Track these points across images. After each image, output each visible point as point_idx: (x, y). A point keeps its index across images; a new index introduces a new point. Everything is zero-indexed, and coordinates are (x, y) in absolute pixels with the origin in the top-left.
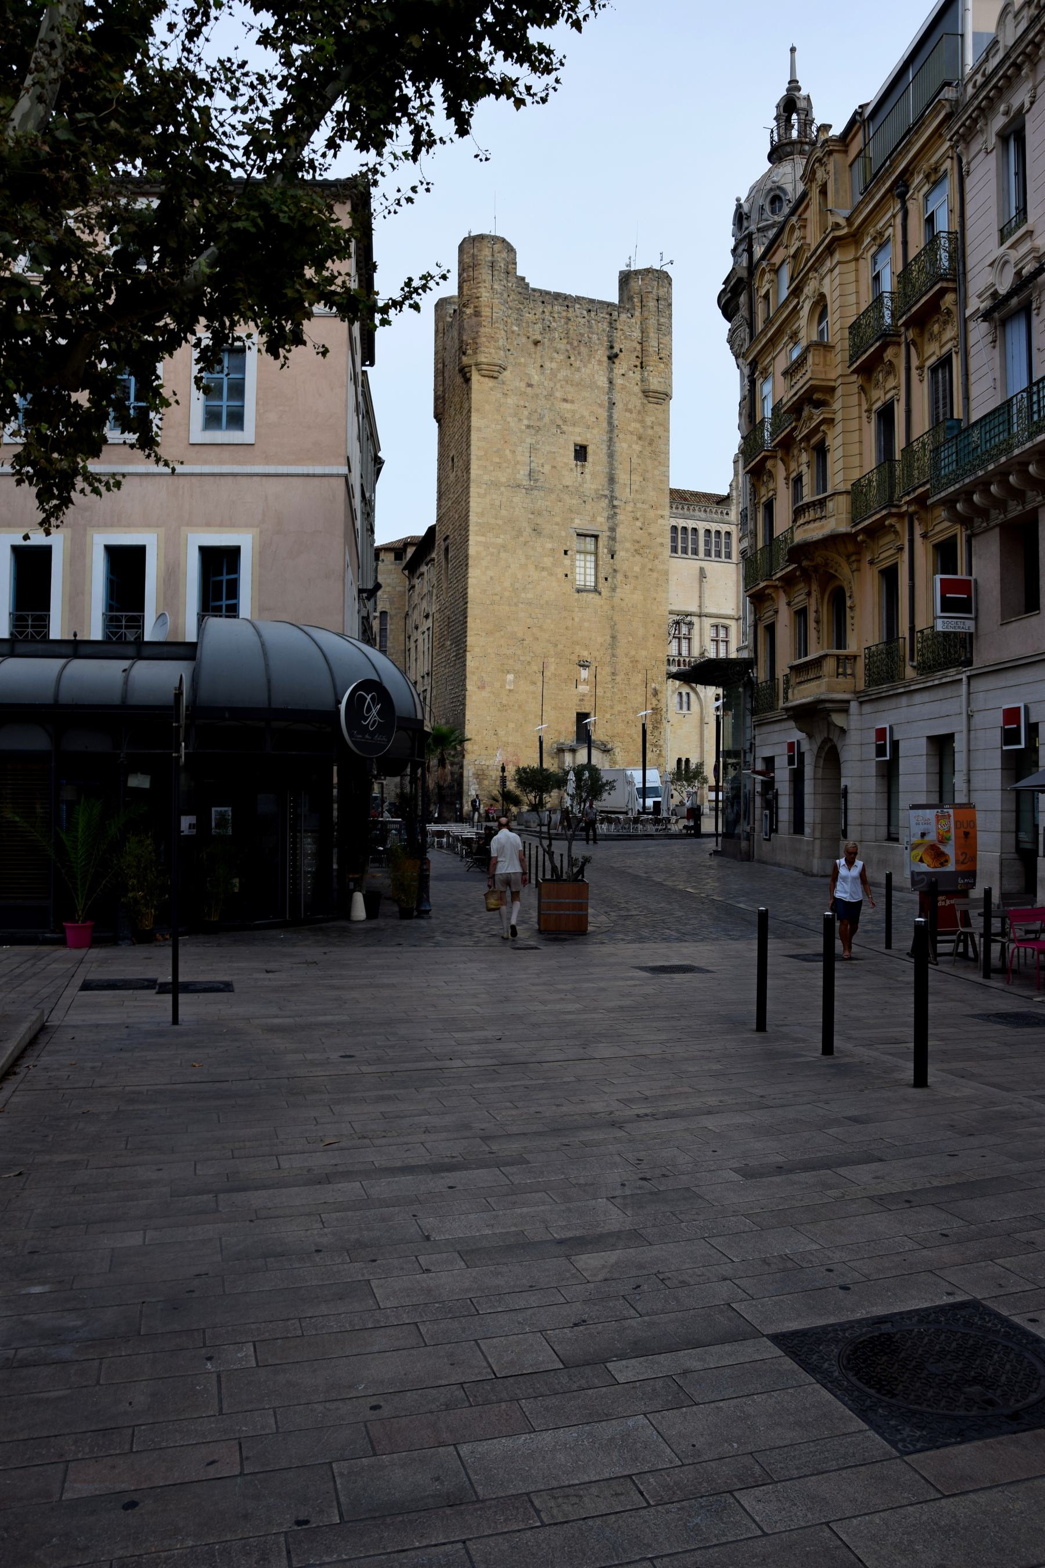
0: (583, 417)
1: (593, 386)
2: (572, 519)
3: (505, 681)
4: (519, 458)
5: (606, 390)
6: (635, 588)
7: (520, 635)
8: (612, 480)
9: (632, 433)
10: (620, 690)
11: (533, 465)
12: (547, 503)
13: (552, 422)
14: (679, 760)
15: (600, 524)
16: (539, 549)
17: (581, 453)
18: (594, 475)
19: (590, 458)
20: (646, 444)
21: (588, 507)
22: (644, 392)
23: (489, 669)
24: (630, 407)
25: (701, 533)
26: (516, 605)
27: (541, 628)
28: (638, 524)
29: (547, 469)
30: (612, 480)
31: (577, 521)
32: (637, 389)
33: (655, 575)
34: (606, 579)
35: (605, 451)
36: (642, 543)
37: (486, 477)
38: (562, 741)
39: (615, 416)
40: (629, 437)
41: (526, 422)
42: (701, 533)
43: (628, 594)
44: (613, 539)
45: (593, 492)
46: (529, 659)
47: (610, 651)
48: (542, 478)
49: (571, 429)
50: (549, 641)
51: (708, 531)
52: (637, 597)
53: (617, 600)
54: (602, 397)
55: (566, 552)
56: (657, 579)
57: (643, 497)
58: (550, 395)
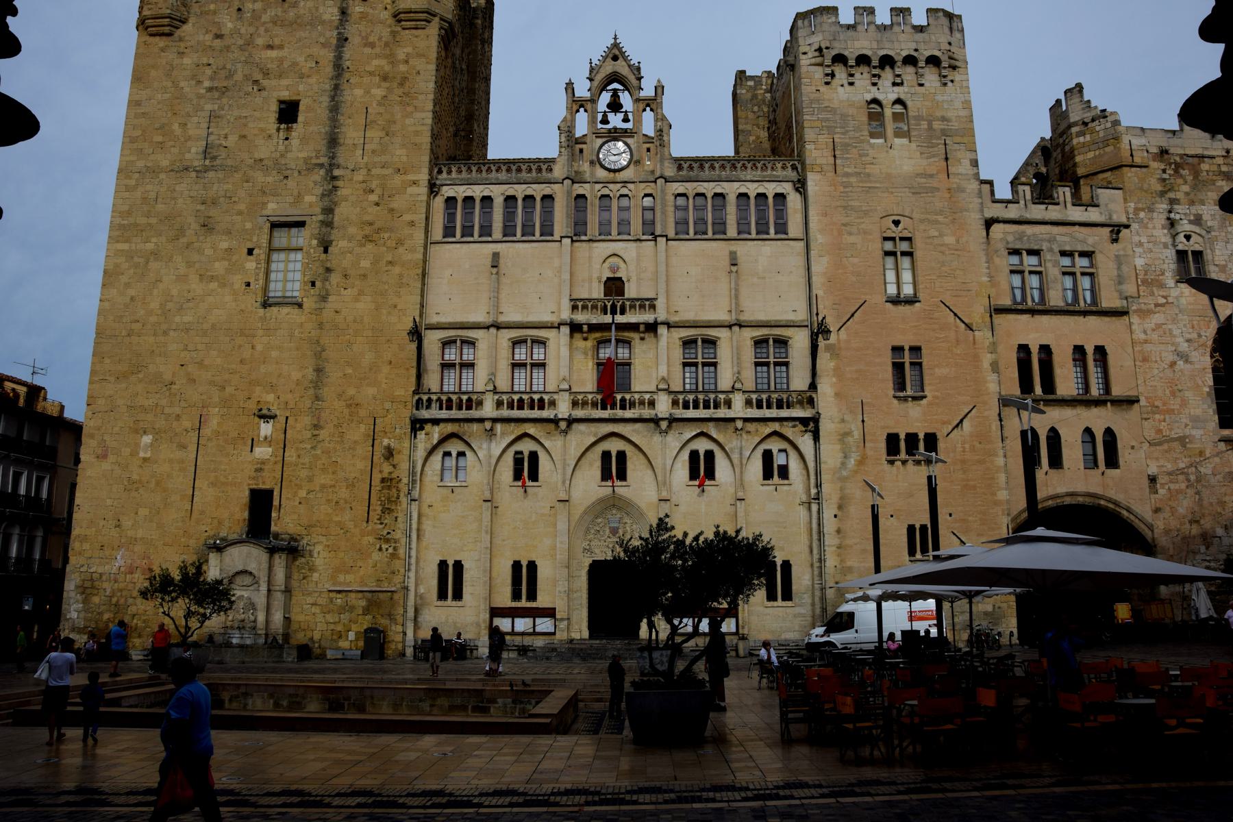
0: (295, 64)
1: (315, 21)
2: (264, 204)
3: (137, 445)
4: (191, 132)
5: (336, 23)
6: (361, 293)
7: (168, 377)
8: (333, 142)
9: (371, 74)
10: (326, 452)
11: (211, 138)
12: (226, 187)
13: (247, 78)
17: (288, 113)
18: (304, 140)
19: (301, 118)
20: (395, 85)
21: (291, 183)
22: (395, 16)
23: (116, 429)
24: (371, 39)
25: (498, 202)
26: (165, 333)
27: (200, 364)
28: (373, 198)
29: (232, 140)
30: (333, 142)
31: (271, 206)
32: (386, 15)
33: (397, 270)
34: (313, 284)
35: (325, 104)
36: (376, 226)
37: (141, 164)
38: (222, 534)
39: (346, 56)
40: (366, 80)
41: (207, 84)
42: (498, 202)
43: (349, 304)
44: (329, 224)
46: (177, 410)
47: (311, 391)
49: (274, 82)
51: (510, 199)
52: (365, 305)
53: (328, 314)
54: (328, 34)
55: (250, 252)
56: (401, 276)
57: (383, 158)
58: (249, 43)
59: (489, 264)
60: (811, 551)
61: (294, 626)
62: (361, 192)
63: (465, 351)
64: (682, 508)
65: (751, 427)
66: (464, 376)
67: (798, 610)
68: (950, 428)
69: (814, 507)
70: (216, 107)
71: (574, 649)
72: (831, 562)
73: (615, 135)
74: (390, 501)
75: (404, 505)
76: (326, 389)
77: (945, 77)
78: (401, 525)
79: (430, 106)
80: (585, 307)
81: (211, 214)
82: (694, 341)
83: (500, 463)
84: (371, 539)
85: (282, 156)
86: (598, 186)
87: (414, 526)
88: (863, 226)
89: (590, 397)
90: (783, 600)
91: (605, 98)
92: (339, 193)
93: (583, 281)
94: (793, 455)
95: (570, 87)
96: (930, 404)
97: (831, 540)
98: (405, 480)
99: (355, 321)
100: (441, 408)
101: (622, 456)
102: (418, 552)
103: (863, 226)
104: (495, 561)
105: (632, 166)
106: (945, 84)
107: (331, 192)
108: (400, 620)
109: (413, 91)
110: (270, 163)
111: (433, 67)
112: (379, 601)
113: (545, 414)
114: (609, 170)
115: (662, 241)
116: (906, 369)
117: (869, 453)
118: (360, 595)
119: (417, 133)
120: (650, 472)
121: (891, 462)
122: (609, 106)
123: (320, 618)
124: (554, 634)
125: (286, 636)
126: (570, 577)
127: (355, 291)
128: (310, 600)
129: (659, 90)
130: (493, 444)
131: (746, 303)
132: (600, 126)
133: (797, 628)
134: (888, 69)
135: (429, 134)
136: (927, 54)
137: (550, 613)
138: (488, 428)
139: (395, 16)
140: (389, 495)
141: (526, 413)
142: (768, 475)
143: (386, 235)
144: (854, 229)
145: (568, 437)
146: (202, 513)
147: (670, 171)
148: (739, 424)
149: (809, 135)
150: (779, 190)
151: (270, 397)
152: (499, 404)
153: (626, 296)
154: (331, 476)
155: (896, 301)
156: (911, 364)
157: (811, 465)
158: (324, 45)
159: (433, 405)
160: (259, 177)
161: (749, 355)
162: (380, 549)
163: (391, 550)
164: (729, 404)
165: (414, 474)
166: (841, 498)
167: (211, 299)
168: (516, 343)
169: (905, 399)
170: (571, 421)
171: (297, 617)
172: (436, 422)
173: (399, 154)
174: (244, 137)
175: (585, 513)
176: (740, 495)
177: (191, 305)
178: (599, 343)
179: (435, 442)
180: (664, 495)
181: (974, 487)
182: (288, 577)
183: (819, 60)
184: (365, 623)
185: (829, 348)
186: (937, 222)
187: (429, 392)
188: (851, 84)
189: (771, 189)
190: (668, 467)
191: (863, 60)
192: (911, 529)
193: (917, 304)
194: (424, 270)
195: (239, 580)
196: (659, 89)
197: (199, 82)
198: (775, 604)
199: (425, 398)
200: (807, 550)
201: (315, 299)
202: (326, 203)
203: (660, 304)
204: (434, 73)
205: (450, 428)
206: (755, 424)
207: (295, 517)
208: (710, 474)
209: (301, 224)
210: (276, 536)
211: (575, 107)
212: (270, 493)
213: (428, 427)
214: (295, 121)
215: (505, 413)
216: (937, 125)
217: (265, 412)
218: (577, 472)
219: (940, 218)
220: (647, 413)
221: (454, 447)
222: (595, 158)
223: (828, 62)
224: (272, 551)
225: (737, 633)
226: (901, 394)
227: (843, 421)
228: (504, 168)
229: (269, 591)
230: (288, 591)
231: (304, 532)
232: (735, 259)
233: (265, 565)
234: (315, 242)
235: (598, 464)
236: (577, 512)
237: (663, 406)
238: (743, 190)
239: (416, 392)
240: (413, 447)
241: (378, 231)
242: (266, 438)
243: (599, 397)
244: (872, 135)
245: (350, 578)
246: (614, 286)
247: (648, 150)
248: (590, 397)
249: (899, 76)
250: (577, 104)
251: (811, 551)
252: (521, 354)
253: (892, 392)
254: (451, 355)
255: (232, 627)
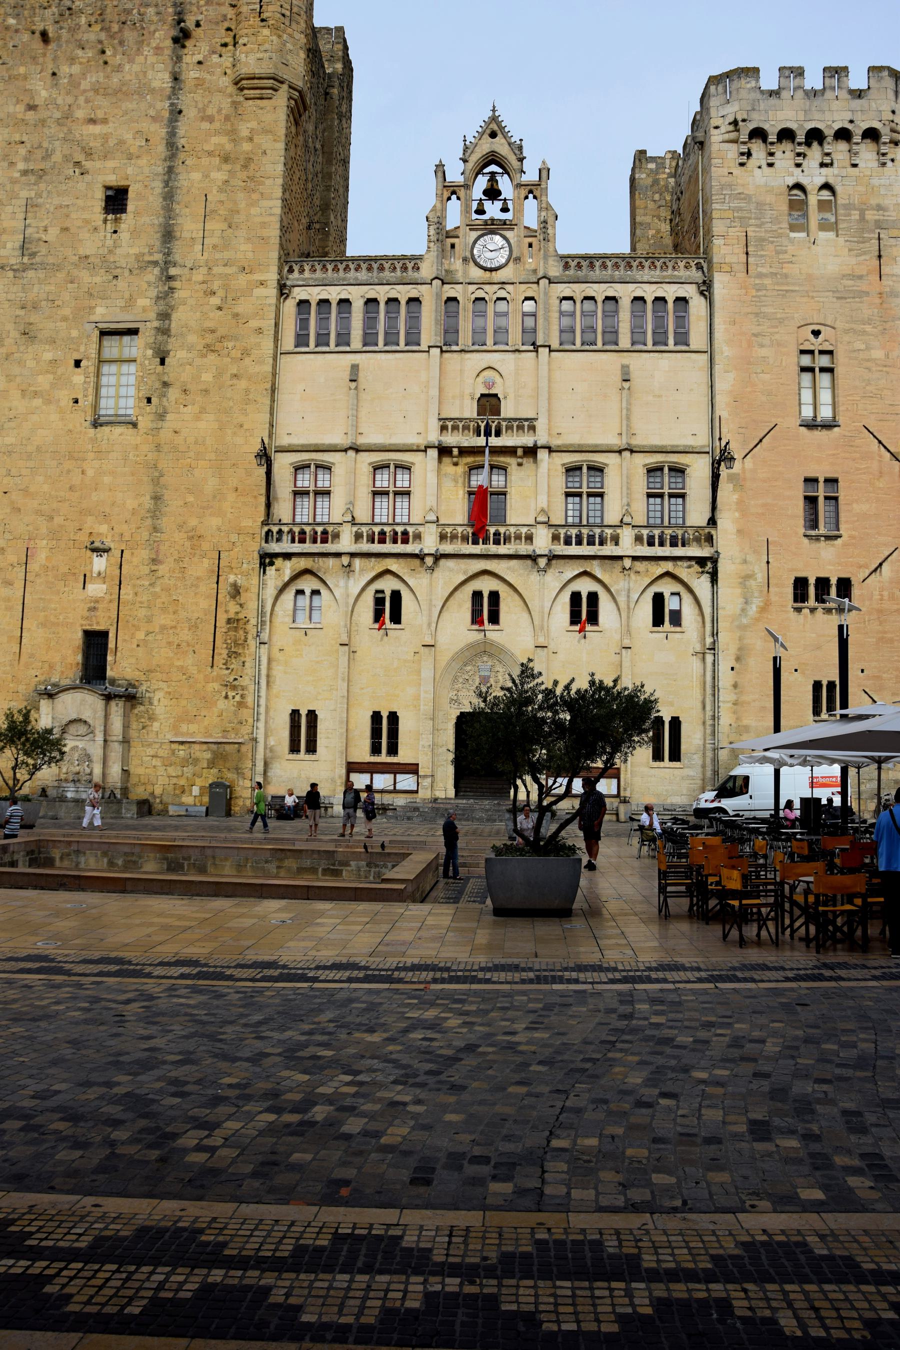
0: (121, 142)
2: (92, 308)
6: (203, 410)
8: (168, 235)
9: (210, 154)
11: (29, 231)
12: (47, 288)
13: (67, 158)
14: (295, 714)
15: (143, 310)
16: (31, 364)
17: (116, 200)
18: (135, 233)
19: (130, 207)
21: (121, 284)
22: (236, 84)
24: (209, 112)
25: (358, 306)
27: (25, 491)
28: (215, 301)
29: (53, 234)
30: (168, 235)
31: (100, 310)
32: (225, 82)
33: (243, 384)
34: (149, 400)
36: (219, 334)
38: (55, 679)
39: (181, 132)
40: (205, 161)
42: (358, 306)
43: (189, 423)
44: (165, 332)
45: (132, 259)
47: (149, 522)
48: (43, 250)
49: (98, 164)
50: (39, 513)
52: (207, 425)
53: (165, 434)
54: (159, 105)
55: (78, 364)
56: (247, 391)
57: (227, 255)
59: (348, 378)
60: (704, 708)
61: (133, 780)
62: (201, 294)
63: (320, 477)
64: (561, 656)
65: (640, 566)
66: (319, 504)
67: (687, 772)
68: (867, 573)
69: (709, 658)
70: (33, 194)
71: (438, 809)
72: (726, 719)
73: (493, 227)
74: (237, 644)
75: (253, 649)
76: (165, 519)
77: (884, 154)
78: (249, 670)
79: (279, 194)
80: (455, 428)
81: (32, 320)
82: (580, 468)
83: (359, 603)
84: (216, 686)
85: (110, 252)
86: (472, 288)
87: (264, 672)
88: (777, 337)
89: (460, 529)
90: (671, 760)
91: (482, 183)
92: (176, 295)
93: (454, 397)
94: (686, 597)
95: (440, 169)
96: (844, 545)
97: (726, 696)
98: (253, 621)
99: (196, 443)
100: (293, 541)
101: (494, 597)
102: (267, 700)
103: (777, 337)
104: (352, 712)
105: (511, 264)
106: (884, 164)
107: (166, 294)
108: (248, 774)
109: (258, 174)
110: (97, 261)
111: (281, 146)
112: (224, 753)
113: (410, 548)
114: (485, 269)
115: (544, 352)
116: (819, 503)
117: (773, 598)
118: (205, 747)
119: (264, 225)
120: (526, 615)
121: (798, 610)
122: (485, 193)
123: (161, 771)
124: (417, 792)
125: (125, 790)
126: (435, 730)
127: (196, 409)
128: (150, 751)
129: (544, 173)
130: (351, 582)
131: (639, 425)
132: (475, 216)
133: (685, 792)
134: (815, 144)
135: (278, 226)
136: (865, 126)
137: (412, 769)
138: (346, 564)
139: (236, 84)
140: (234, 637)
141: (388, 547)
142: (658, 620)
143: (230, 345)
144: (766, 341)
145: (435, 574)
146: (32, 656)
147: (555, 270)
148: (627, 563)
149: (718, 227)
150: (681, 294)
151: (104, 528)
152: (358, 537)
153: (503, 415)
154: (172, 616)
155: (811, 425)
156: (826, 498)
157: (707, 610)
158: (154, 119)
159: (285, 537)
160: (85, 277)
161: (640, 485)
162: (226, 697)
163: (238, 698)
164: (616, 540)
165: (263, 614)
166: (740, 649)
167: (35, 418)
168: (377, 468)
169: (817, 538)
170: (439, 557)
171: (136, 770)
172: (287, 556)
173: (244, 250)
174: (66, 229)
175: (453, 659)
176: (626, 643)
177: (12, 424)
178: (471, 469)
179: (287, 578)
180: (541, 641)
181: (891, 641)
182: (126, 727)
183: (733, 135)
184: (211, 776)
185: (731, 478)
186: (864, 333)
187: (280, 523)
188: (770, 165)
189: (671, 292)
190: (547, 610)
191: (786, 135)
192: (817, 686)
193: (836, 429)
194: (273, 384)
195: (72, 729)
196: (544, 172)
197: (12, 164)
198: (661, 764)
199: (275, 529)
200: (699, 705)
201: (151, 417)
202: (162, 308)
203: (540, 425)
204: (283, 152)
205: (303, 563)
206: (645, 563)
207: (133, 661)
208: (593, 618)
209: (134, 332)
210: (113, 682)
211: (446, 194)
212: (104, 634)
213: (279, 562)
214: (123, 210)
215: (365, 547)
216: (871, 216)
217: (97, 544)
218: (444, 614)
219: (868, 328)
220: (523, 548)
221: (308, 584)
222: (468, 255)
223: (744, 137)
224: (108, 698)
225: (618, 795)
226: (813, 533)
227: (745, 562)
228: (364, 266)
229: (105, 741)
230: (126, 741)
231: (143, 678)
232: (628, 373)
233: (101, 714)
234: (150, 352)
235: (468, 605)
236: (444, 658)
237: (542, 542)
238: (639, 293)
239: (265, 523)
240: (262, 585)
241: (222, 339)
242: (99, 574)
243: (470, 530)
244: (793, 228)
245: (193, 728)
246: (489, 403)
247: (530, 245)
248: (460, 529)
249: (828, 154)
250: (450, 191)
251: (704, 708)
252: (383, 480)
253: (802, 530)
254: (305, 481)
255: (66, 780)
